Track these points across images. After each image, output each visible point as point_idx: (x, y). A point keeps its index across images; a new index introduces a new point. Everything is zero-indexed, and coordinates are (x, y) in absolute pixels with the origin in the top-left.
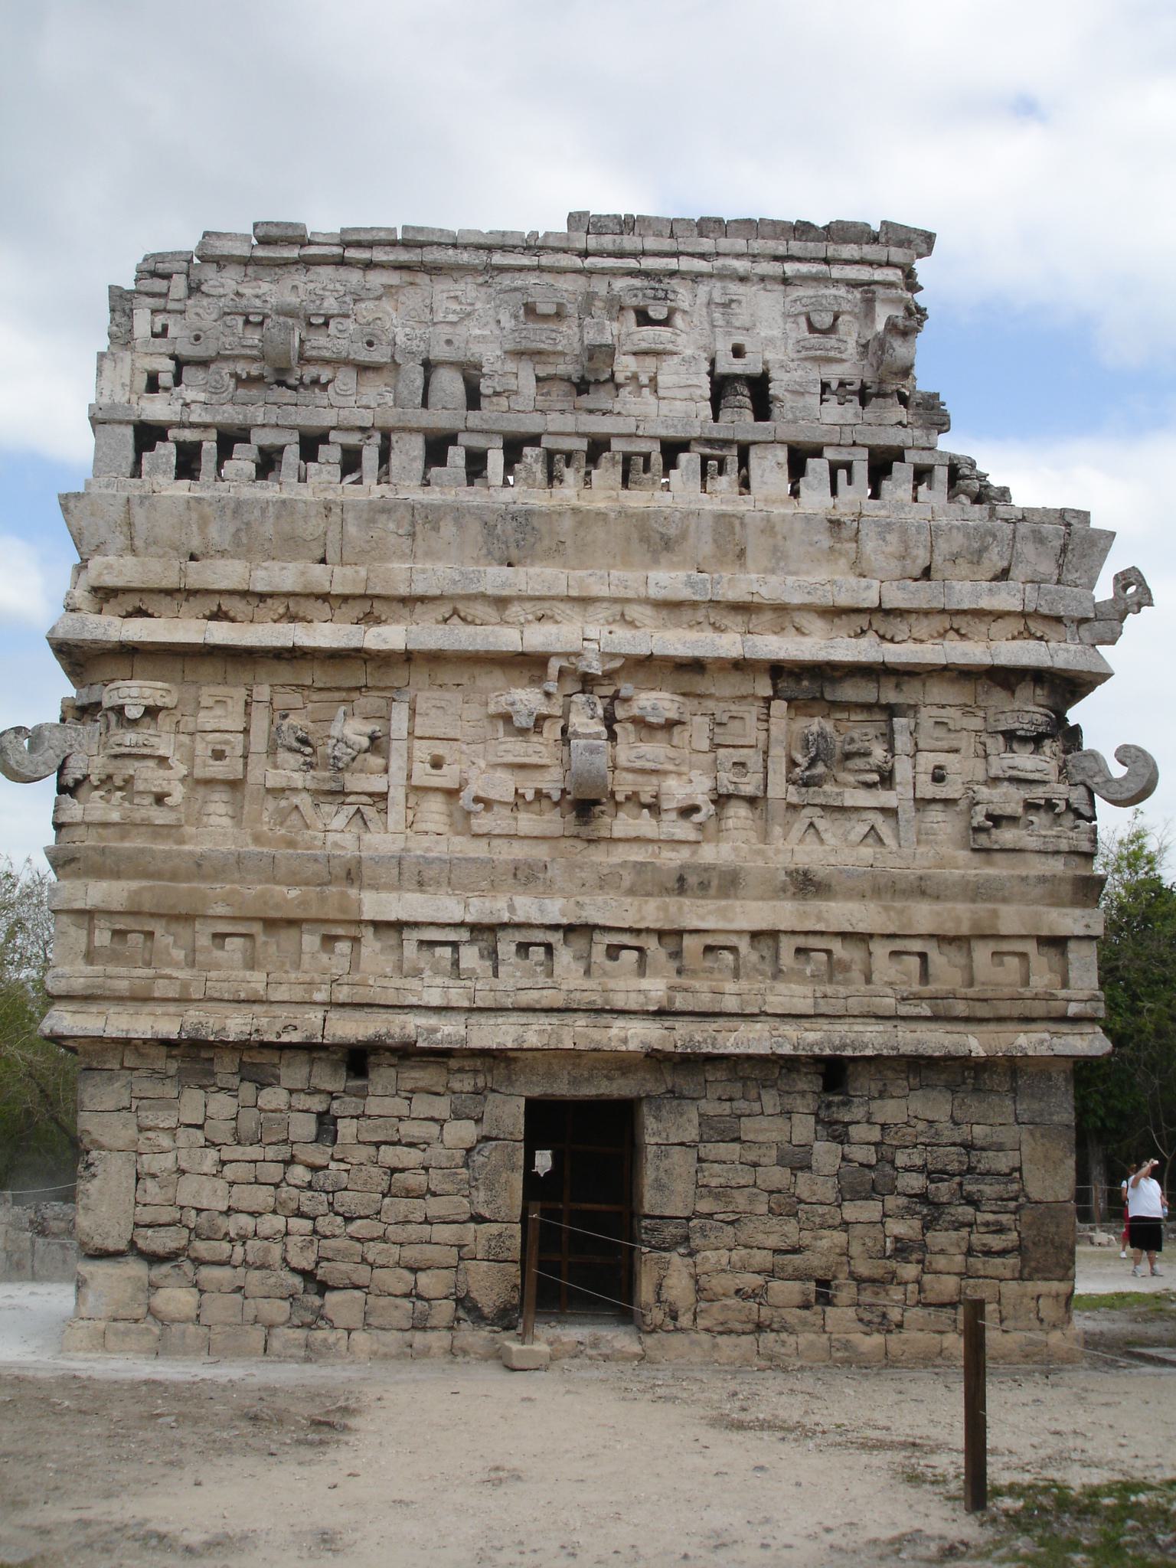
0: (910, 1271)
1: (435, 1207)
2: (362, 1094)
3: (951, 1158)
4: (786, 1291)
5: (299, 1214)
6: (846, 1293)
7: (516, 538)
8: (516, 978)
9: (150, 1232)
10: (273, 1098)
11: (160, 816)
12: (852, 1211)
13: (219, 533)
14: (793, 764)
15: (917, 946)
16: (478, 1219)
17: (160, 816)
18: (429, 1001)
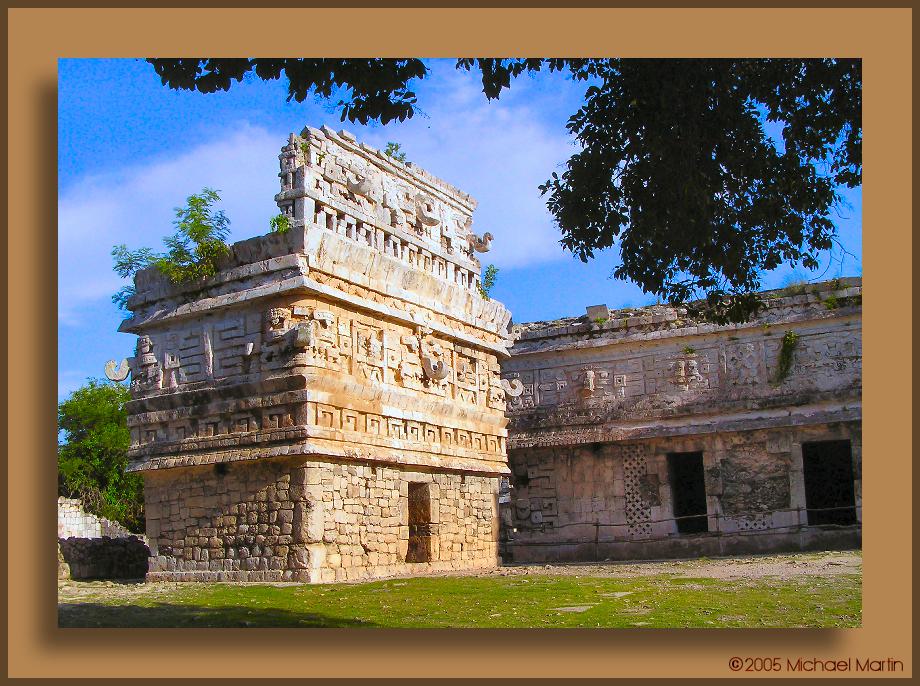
0: (476, 539)
1: (392, 521)
2: (374, 480)
3: (480, 504)
4: (457, 547)
5: (362, 524)
6: (465, 545)
7: (409, 279)
8: (410, 441)
9: (328, 532)
10: (355, 480)
11: (335, 367)
12: (468, 521)
13: (343, 257)
14: (459, 374)
15: (479, 436)
16: (400, 525)
17: (335, 367)
18: (401, 446)
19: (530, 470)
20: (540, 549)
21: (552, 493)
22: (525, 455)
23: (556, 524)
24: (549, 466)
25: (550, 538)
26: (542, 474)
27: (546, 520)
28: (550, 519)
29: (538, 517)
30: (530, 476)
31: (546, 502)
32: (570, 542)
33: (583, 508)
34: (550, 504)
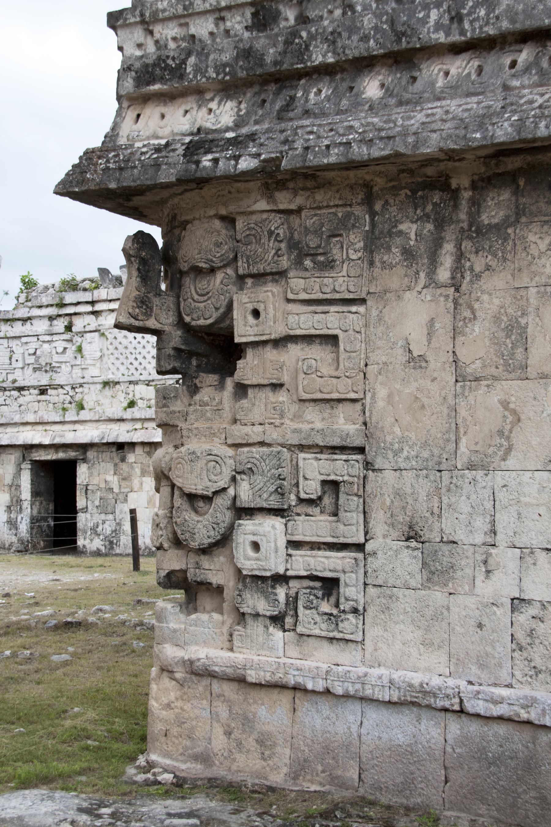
19: (243, 302)
20: (272, 714)
21: (345, 425)
22: (229, 221)
23: (351, 591)
24: (340, 282)
25: (315, 663)
26: (306, 321)
27: (303, 563)
28: (326, 563)
29: (264, 543)
30: (244, 330)
31: (314, 471)
32: (414, 702)
33: (505, 521)
34: (332, 486)
